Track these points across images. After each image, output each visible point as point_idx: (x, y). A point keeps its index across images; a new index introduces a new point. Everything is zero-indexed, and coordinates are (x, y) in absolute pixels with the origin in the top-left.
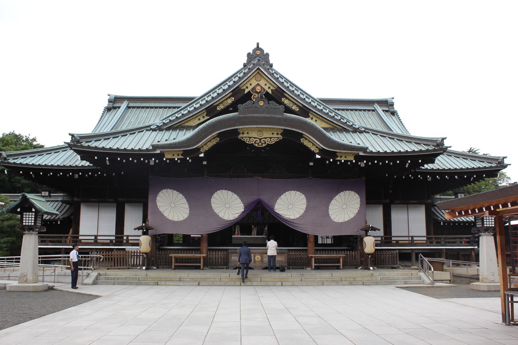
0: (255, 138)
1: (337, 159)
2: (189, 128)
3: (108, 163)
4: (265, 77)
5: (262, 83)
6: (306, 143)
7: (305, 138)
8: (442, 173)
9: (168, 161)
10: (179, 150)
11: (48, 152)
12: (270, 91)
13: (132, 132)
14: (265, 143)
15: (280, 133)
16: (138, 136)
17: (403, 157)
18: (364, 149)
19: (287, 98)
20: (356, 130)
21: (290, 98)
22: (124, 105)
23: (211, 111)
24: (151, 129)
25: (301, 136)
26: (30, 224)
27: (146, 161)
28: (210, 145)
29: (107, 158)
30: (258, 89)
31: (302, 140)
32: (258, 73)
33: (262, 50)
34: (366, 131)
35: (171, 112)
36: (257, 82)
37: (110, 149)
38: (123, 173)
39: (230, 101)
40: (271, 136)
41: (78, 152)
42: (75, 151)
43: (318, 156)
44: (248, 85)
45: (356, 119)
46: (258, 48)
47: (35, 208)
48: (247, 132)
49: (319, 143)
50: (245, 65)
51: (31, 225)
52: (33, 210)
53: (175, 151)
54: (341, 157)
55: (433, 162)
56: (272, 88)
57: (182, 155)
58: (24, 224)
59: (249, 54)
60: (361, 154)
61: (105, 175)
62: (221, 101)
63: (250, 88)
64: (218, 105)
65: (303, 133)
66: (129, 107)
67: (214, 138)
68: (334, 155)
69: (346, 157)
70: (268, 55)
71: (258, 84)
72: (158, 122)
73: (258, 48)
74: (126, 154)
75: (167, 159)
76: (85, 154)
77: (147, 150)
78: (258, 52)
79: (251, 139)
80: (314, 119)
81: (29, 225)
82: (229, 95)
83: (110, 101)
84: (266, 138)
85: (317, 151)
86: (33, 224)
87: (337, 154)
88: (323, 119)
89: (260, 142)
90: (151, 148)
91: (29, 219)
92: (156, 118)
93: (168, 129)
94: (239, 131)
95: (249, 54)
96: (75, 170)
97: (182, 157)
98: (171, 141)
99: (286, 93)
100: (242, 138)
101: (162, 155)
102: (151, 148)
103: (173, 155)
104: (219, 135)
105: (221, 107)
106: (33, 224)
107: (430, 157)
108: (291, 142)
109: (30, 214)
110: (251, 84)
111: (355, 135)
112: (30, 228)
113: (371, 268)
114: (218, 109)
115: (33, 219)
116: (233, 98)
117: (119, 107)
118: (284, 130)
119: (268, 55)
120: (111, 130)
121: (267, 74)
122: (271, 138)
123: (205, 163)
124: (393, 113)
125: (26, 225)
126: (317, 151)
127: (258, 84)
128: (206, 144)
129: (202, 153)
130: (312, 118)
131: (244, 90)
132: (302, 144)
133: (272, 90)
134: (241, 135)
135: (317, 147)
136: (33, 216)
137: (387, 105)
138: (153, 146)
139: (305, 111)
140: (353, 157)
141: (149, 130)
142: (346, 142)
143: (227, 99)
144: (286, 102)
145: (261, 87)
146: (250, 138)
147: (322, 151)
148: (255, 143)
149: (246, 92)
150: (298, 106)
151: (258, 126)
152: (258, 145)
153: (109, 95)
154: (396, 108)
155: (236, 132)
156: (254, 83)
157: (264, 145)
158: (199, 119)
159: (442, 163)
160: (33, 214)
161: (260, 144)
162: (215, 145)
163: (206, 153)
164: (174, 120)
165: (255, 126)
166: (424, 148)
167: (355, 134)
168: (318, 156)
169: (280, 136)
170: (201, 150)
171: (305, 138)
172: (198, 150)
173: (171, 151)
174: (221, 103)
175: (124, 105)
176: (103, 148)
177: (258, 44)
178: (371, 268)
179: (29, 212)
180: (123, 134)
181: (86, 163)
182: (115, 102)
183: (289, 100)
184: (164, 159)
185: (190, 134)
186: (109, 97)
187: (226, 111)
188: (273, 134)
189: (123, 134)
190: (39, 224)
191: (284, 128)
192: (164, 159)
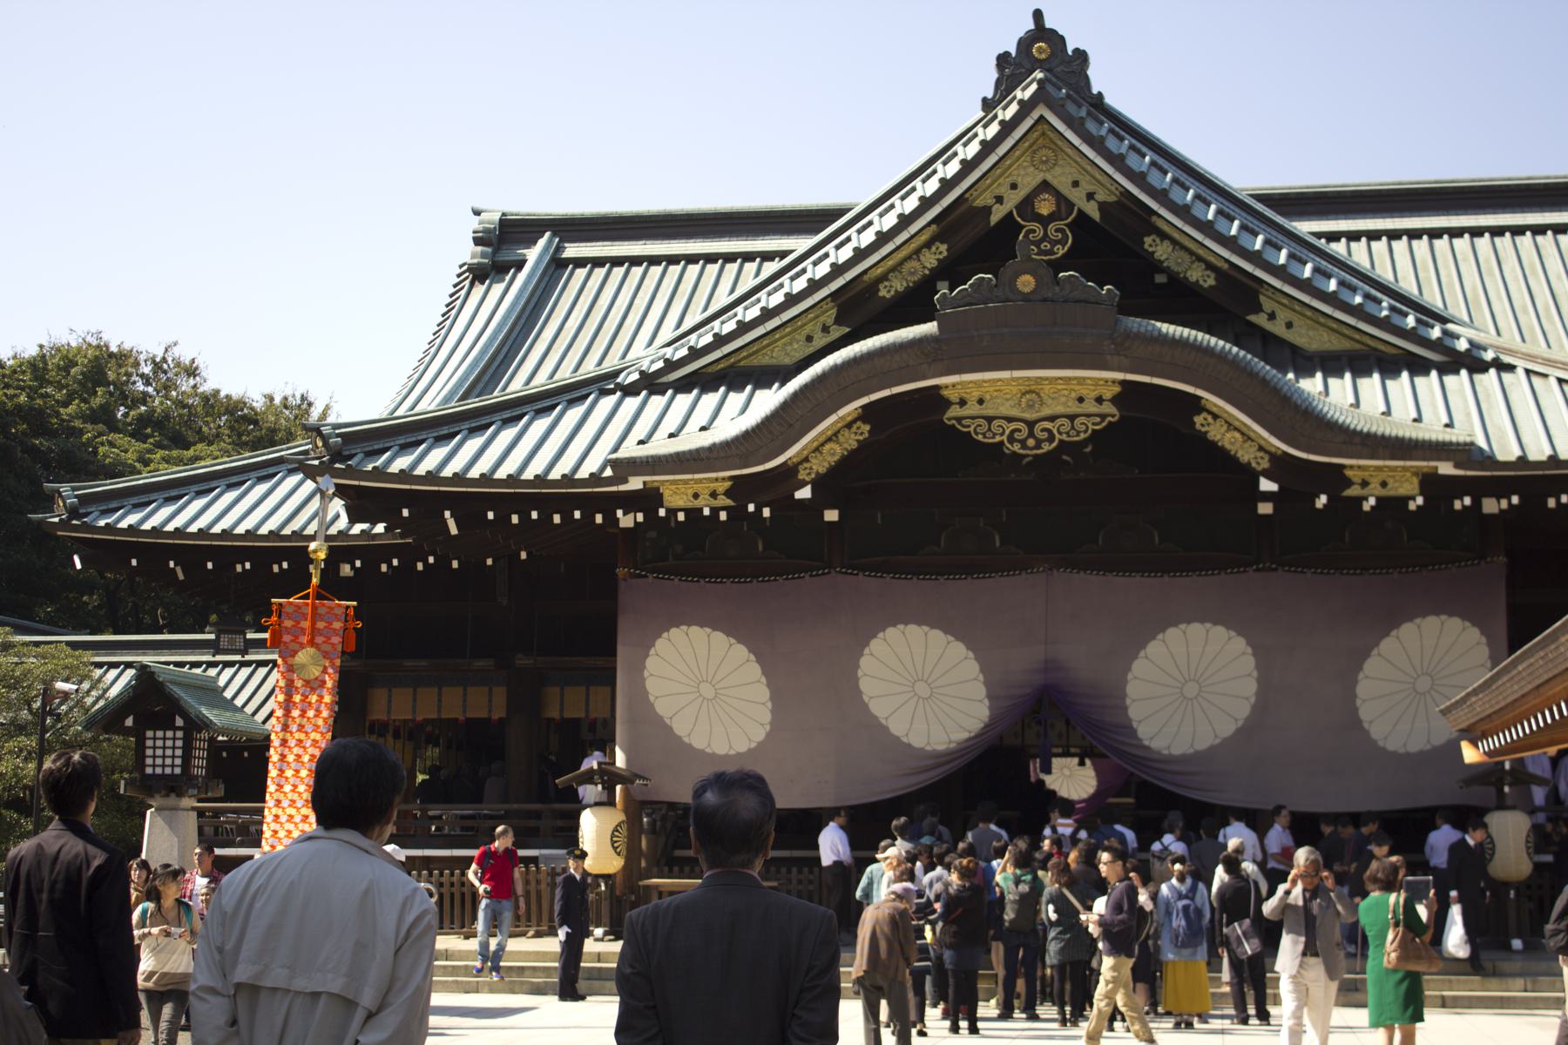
0: (1010, 420)
1: (1349, 492)
3: (454, 530)
4: (1069, 151)
5: (1061, 178)
6: (1216, 432)
7: (1210, 412)
9: (681, 517)
10: (713, 475)
11: (234, 479)
12: (1092, 211)
14: (1051, 439)
15: (1108, 395)
19: (1164, 236)
21: (1176, 235)
24: (620, 387)
25: (1195, 405)
26: (168, 771)
27: (599, 519)
28: (833, 453)
29: (447, 514)
30: (1045, 207)
31: (1198, 420)
32: (1043, 134)
33: (1055, 39)
36: (1039, 178)
38: (523, 555)
39: (930, 260)
40: (1074, 408)
41: (341, 491)
43: (1266, 485)
44: (1004, 190)
46: (1041, 31)
47: (185, 715)
48: (976, 394)
49: (1265, 434)
50: (988, 105)
51: (173, 774)
52: (179, 722)
53: (700, 481)
54: (1365, 484)
56: (1100, 197)
57: (728, 493)
58: (149, 770)
59: (1003, 59)
60: (1446, 468)
61: (455, 564)
62: (890, 263)
63: (1012, 200)
64: (884, 278)
65: (1200, 393)
66: (557, 266)
67: (849, 426)
68: (1334, 478)
69: (1384, 484)
70: (1081, 56)
71: (1045, 186)
72: (646, 357)
73: (1041, 31)
75: (672, 512)
76: (361, 504)
77: (595, 478)
78: (1040, 49)
79: (996, 423)
80: (1283, 315)
81: (163, 775)
82: (924, 238)
84: (1052, 419)
85: (1265, 464)
86: (178, 771)
87: (1348, 473)
89: (1031, 434)
90: (608, 472)
91: (164, 752)
93: (683, 386)
94: (945, 393)
95: (1003, 59)
97: (729, 502)
98: (692, 440)
99: (1160, 216)
100: (959, 420)
101: (648, 499)
102: (608, 472)
103: (696, 496)
104: (867, 413)
105: (895, 286)
106: (178, 771)
108: (1152, 430)
109: (169, 734)
110: (1014, 186)
112: (172, 786)
113: (1517, 944)
114: (883, 293)
115: (179, 752)
116: (943, 248)
117: (520, 265)
118: (1123, 383)
119: (1081, 56)
120: (464, 397)
121: (1076, 140)
122: (1072, 418)
123: (831, 515)
125: (154, 775)
126: (1265, 464)
127: (1045, 186)
128: (817, 450)
129: (803, 484)
130: (1272, 316)
131: (987, 210)
132: (1203, 436)
133: (1102, 206)
134: (955, 411)
135: (1261, 448)
136: (179, 743)
138: (614, 464)
140: (1416, 481)
141: (612, 392)
142: (1401, 424)
143: (918, 252)
144: (1162, 251)
145: (1060, 197)
146: (990, 419)
147: (1280, 466)
148: (1011, 439)
149: (995, 219)
150: (1210, 266)
151: (1017, 374)
152: (1023, 443)
153: (477, 213)
155: (934, 400)
157: (1046, 447)
158: (809, 339)
160: (180, 734)
161: (1031, 442)
162: (852, 453)
163: (818, 484)
164: (708, 349)
165: (1005, 374)
167: (1450, 380)
168: (1266, 485)
169: (1108, 408)
170: (802, 475)
171: (1210, 412)
172: (788, 475)
173: (686, 482)
174: (893, 269)
177: (1038, 15)
178: (1517, 944)
179: (165, 730)
180: (507, 414)
182: (502, 242)
183: (1174, 242)
184: (662, 512)
185: (768, 400)
186: (474, 223)
187: (912, 306)
188: (1081, 400)
189: (507, 414)
190: (199, 766)
191: (1120, 376)
192: (662, 512)
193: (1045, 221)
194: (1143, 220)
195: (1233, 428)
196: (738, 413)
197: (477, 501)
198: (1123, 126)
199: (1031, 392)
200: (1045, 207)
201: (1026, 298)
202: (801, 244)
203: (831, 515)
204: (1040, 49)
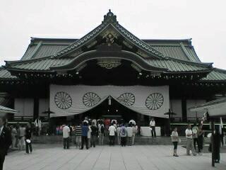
2: (72, 58)
5: (112, 33)
8: (214, 82)
13: (40, 60)
16: (43, 62)
17: (188, 74)
18: (166, 70)
20: (163, 59)
22: (39, 44)
23: (84, 48)
30: (110, 35)
34: (170, 59)
35: (63, 48)
37: (27, 69)
39: (94, 43)
42: (9, 71)
45: (164, 52)
55: (206, 77)
59: (105, 16)
66: (42, 45)
68: (149, 73)
70: (115, 16)
72: (55, 55)
74: (35, 72)
76: (13, 73)
83: (31, 41)
88: (146, 53)
92: (55, 51)
93: (60, 59)
96: (10, 80)
101: (55, 73)
105: (89, 47)
107: (205, 74)
111: (162, 62)
124: (192, 48)
132: (133, 69)
137: (187, 43)
139: (135, 49)
144: (125, 43)
147: (142, 71)
154: (192, 44)
156: (108, 33)
159: (211, 77)
166: (200, 69)
172: (75, 71)
175: (39, 44)
176: (23, 69)
181: (15, 77)
182: (34, 42)
185: (71, 61)
187: (92, 48)
193: (110, 39)
194: (123, 39)
195: (137, 67)
196: (67, 62)
197: (29, 72)
198: (121, 26)
199: (108, 60)
200: (110, 35)
201: (110, 47)
202: (71, 44)
203: (80, 77)
204: (110, 15)
